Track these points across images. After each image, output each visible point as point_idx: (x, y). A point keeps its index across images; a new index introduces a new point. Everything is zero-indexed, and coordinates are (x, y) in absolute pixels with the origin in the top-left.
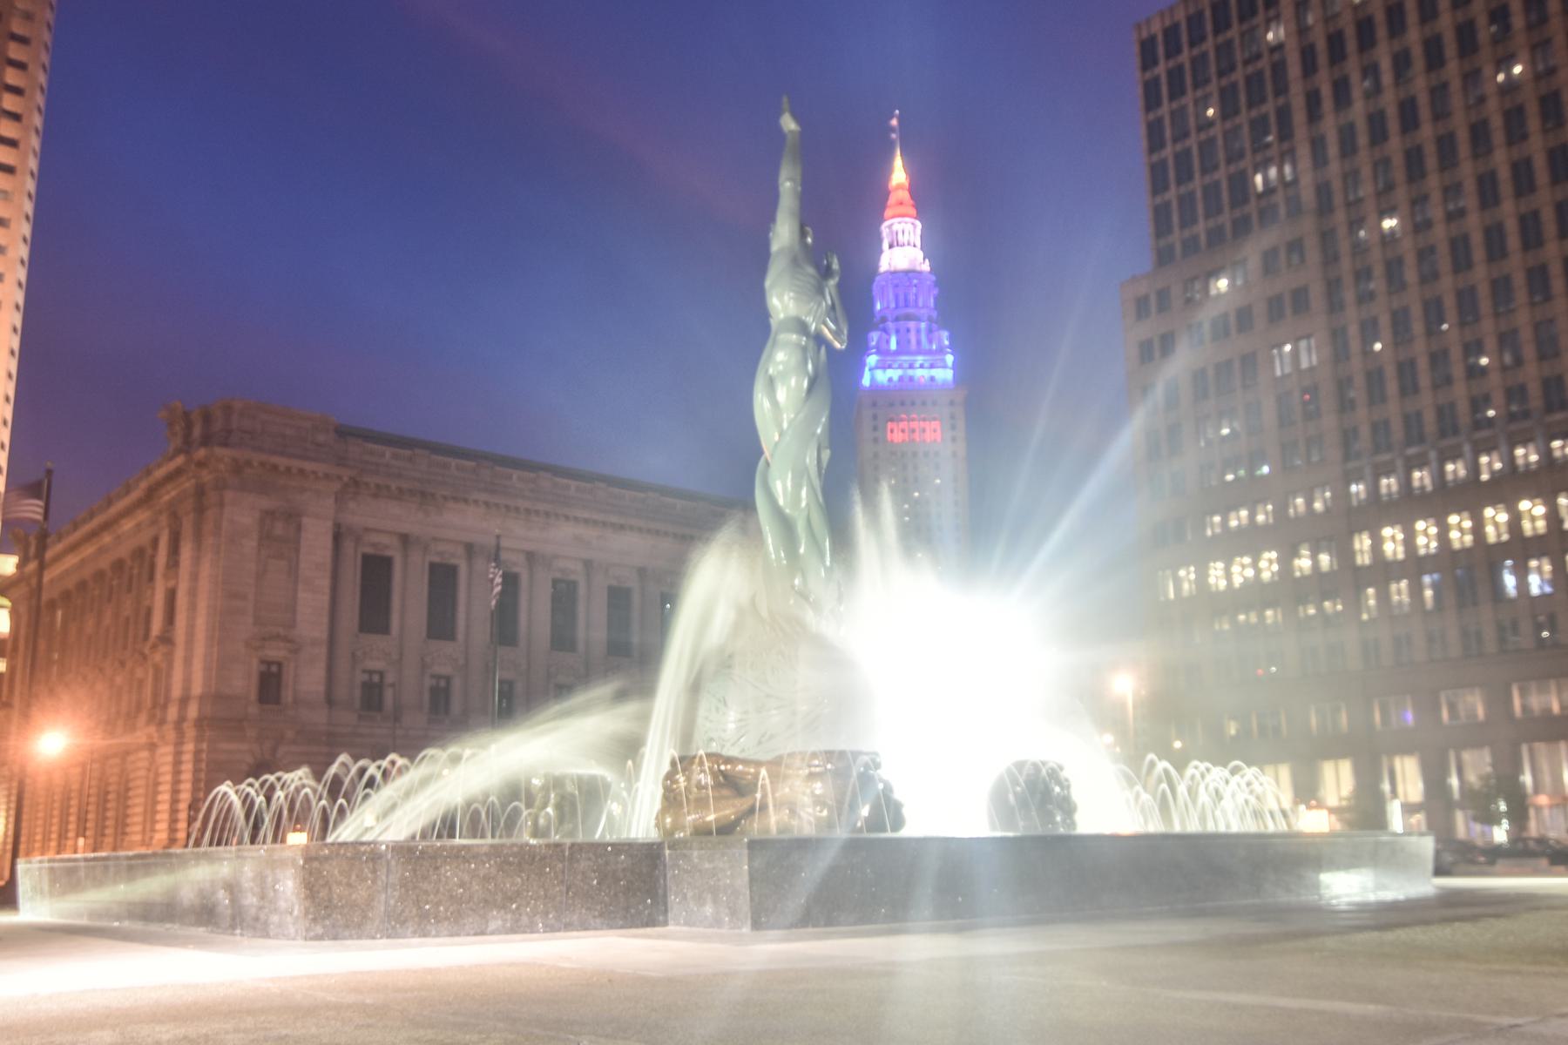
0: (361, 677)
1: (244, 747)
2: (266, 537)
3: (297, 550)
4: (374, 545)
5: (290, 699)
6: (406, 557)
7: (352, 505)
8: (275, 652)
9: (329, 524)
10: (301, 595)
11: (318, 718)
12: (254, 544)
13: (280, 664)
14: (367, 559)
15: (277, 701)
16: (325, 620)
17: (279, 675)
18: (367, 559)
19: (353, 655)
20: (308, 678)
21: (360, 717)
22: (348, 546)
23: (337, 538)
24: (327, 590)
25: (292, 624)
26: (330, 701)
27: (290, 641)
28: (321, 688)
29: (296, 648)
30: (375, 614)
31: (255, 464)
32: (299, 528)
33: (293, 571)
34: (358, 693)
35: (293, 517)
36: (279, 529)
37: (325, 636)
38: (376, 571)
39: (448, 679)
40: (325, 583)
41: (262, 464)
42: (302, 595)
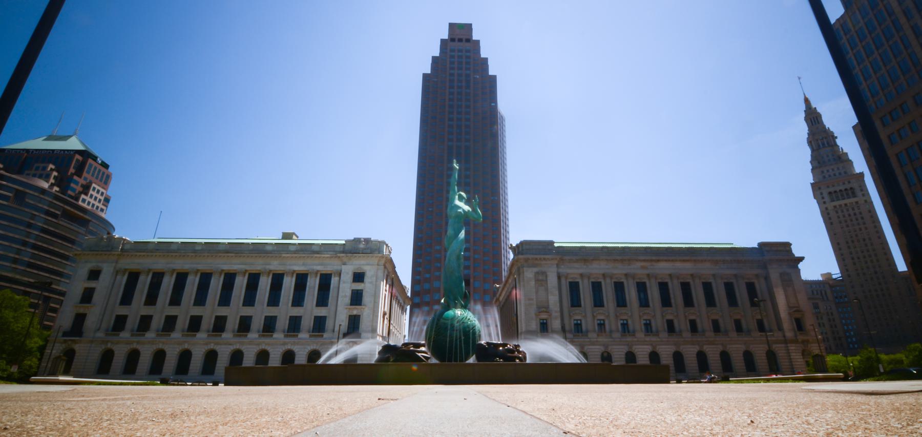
0: (573, 323)
2: (537, 280)
3: (547, 284)
4: (572, 278)
7: (562, 267)
8: (544, 316)
9: (556, 274)
10: (549, 297)
12: (534, 283)
13: (546, 320)
14: (571, 283)
16: (558, 304)
17: (546, 323)
18: (571, 283)
20: (556, 324)
22: (563, 281)
23: (559, 277)
24: (557, 294)
28: (560, 327)
30: (575, 301)
33: (547, 290)
35: (544, 274)
37: (559, 309)
38: (574, 288)
39: (604, 320)
40: (557, 292)
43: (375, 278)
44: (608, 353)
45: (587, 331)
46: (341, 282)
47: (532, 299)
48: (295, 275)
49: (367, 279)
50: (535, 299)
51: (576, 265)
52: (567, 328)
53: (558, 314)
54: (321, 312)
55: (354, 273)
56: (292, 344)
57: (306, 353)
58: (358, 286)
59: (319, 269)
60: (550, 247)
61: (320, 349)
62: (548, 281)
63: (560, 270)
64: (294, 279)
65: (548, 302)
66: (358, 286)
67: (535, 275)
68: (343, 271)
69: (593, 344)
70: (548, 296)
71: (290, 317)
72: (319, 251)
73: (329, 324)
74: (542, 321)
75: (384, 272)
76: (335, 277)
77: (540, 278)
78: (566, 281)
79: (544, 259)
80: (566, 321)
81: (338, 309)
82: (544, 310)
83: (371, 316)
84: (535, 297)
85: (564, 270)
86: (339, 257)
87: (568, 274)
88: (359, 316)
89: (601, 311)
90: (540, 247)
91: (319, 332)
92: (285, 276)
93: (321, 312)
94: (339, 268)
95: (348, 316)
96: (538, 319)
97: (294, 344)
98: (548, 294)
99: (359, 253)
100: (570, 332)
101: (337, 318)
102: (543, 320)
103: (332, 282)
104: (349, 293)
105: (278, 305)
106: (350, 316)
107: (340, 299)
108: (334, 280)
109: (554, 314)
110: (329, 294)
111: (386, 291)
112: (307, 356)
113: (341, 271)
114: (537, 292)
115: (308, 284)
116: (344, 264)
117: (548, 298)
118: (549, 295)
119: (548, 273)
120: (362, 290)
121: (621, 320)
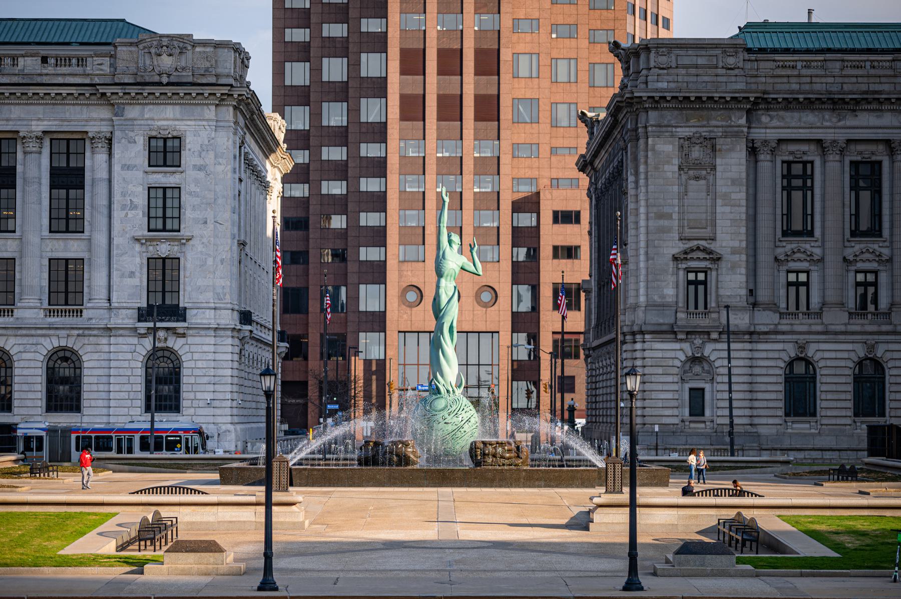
1: (677, 346)
5: (713, 305)
6: (824, 162)
7: (765, 119)
10: (719, 209)
12: (676, 168)
16: (743, 230)
17: (705, 283)
23: (753, 151)
24: (744, 203)
25: (713, 239)
27: (711, 252)
28: (743, 292)
33: (711, 191)
36: (696, 153)
39: (876, 273)
40: (740, 196)
43: (211, 155)
47: (669, 216)
49: (188, 158)
50: (675, 216)
51: (810, 117)
52: (763, 295)
63: (759, 134)
68: (117, 134)
70: (714, 206)
74: (692, 276)
81: (116, 241)
82: (703, 243)
84: (677, 209)
86: (104, 94)
95: (145, 262)
96: (681, 273)
101: (114, 266)
104: (141, 200)
107: (117, 214)
118: (719, 202)
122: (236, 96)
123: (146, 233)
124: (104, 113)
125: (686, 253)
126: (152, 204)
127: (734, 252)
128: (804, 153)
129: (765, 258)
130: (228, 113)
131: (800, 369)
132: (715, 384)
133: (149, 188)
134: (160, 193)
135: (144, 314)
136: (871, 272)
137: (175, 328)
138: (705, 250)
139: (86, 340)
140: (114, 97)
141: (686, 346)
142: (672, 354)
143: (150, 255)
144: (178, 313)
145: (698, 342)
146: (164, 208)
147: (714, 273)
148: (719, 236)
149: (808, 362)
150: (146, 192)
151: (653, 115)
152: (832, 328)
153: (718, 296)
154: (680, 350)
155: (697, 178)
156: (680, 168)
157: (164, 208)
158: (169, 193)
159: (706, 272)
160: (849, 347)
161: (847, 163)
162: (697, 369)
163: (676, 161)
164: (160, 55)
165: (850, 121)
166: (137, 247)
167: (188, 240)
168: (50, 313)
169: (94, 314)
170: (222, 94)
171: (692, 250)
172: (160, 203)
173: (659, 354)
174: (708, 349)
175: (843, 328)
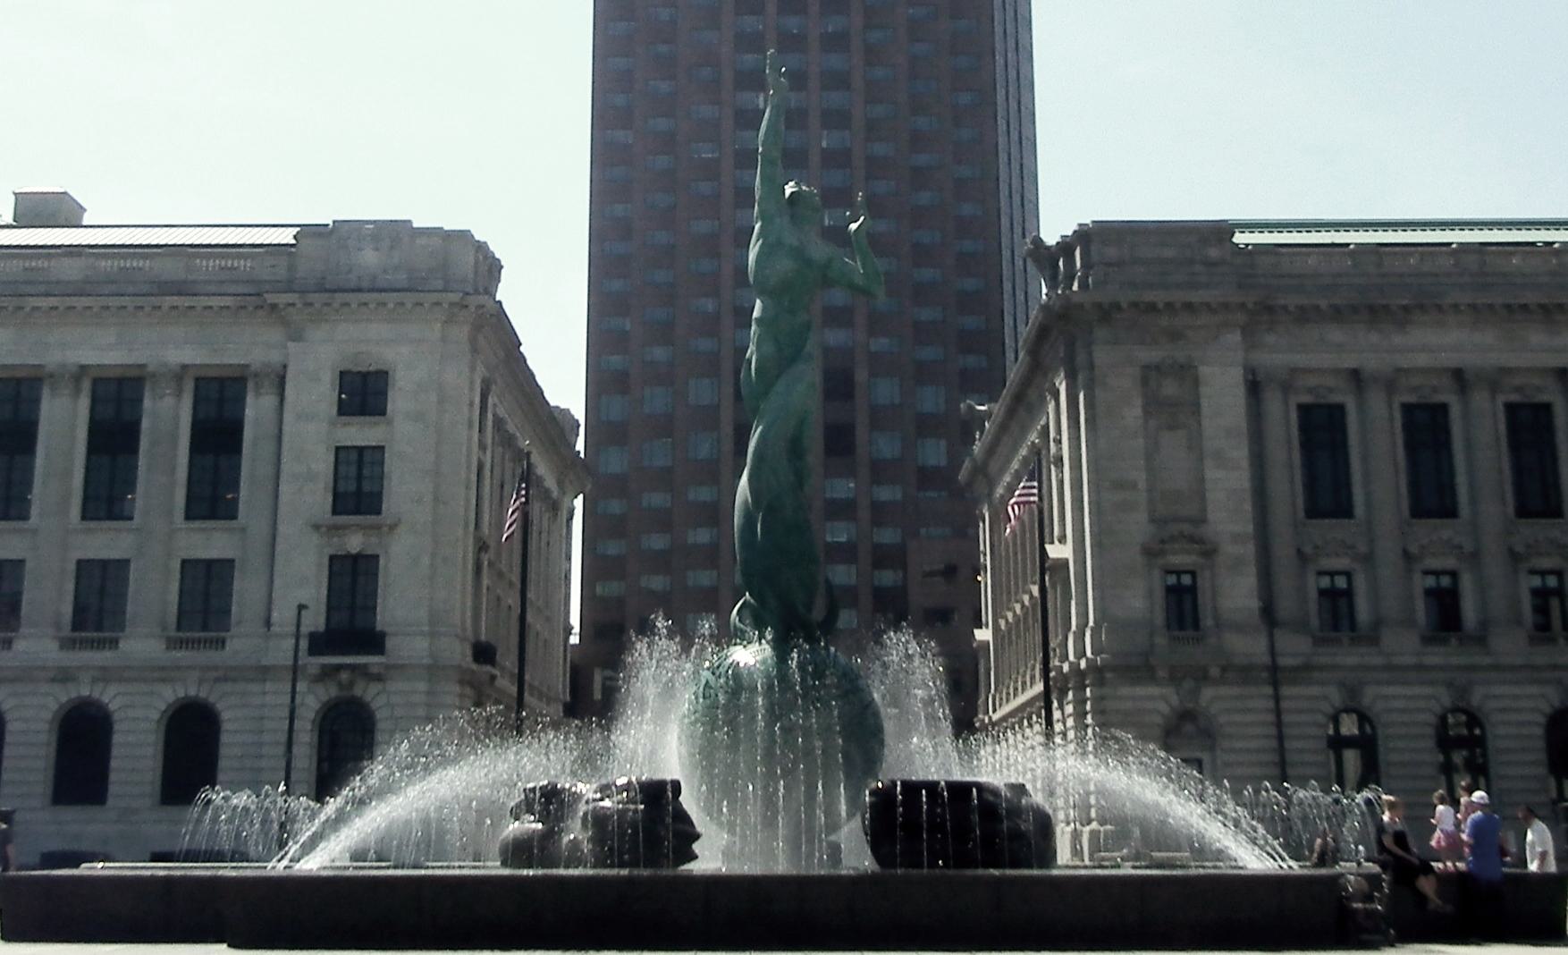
0: (1314, 584)
1: (1153, 690)
2: (1153, 405)
7: (1270, 339)
11: (1251, 647)
12: (1138, 411)
13: (1193, 574)
15: (1196, 625)
17: (1193, 590)
19: (1299, 552)
21: (1319, 642)
23: (1254, 387)
24: (1245, 464)
25: (1201, 520)
26: (1269, 615)
27: (1201, 541)
28: (1255, 604)
29: (1209, 552)
31: (1124, 305)
32: (1196, 382)
34: (1313, 607)
35: (1187, 373)
36: (1170, 388)
37: (1250, 528)
41: (1135, 305)
42: (1212, 473)
43: (433, 398)
44: (1474, 720)
45: (1378, 624)
46: (288, 417)
47: (1134, 486)
48: (86, 385)
49: (398, 401)
50: (1142, 485)
51: (1336, 334)
52: (1286, 606)
53: (1249, 550)
54: (211, 542)
55: (342, 373)
56: (94, 681)
57: (155, 716)
58: (360, 433)
59: (187, 361)
60: (1214, 253)
61: (212, 700)
62: (1204, 403)
64: (84, 404)
65: (1200, 494)
66: (360, 433)
67: (1145, 381)
69: (1395, 672)
71: (79, 562)
72: (185, 282)
73: (246, 592)
74: (1172, 580)
75: (473, 369)
76: (258, 394)
77: (1170, 388)
78: (1286, 403)
79: (1189, 307)
80: (1285, 582)
81: (281, 528)
82: (1187, 528)
83: (426, 560)
85: (1278, 353)
87: (1294, 371)
88: (378, 556)
89: (1446, 534)
90: (1169, 253)
91: (205, 628)
92: (46, 393)
93: (211, 542)
94: (275, 357)
95: (326, 561)
96: (1157, 574)
97: (105, 675)
98: (1201, 459)
99: (359, 290)
100: (1301, 626)
101: (278, 567)
102: (1178, 573)
103: (249, 412)
104: (323, 465)
105: (24, 516)
106: (332, 558)
108: (256, 409)
109: (1229, 549)
110: (238, 467)
111: (482, 447)
112: (163, 728)
113: (285, 367)
114: (1150, 455)
115: (145, 424)
116: (297, 336)
117: (1202, 480)
118: (1208, 463)
119: (1204, 370)
120: (381, 449)
121: (1533, 572)
122: (473, 309)
123: (328, 515)
124: (275, 335)
125: (1163, 542)
126: (342, 469)
127: (1237, 538)
128: (1331, 390)
129: (1283, 550)
130: (461, 333)
131: (1349, 727)
132: (1219, 753)
133: (338, 449)
134: (354, 456)
135: (320, 644)
136: (1444, 572)
137: (365, 666)
138: (1192, 539)
139: (227, 687)
140: (291, 309)
141: (1169, 691)
142: (1150, 705)
143: (333, 552)
144: (373, 641)
145: (1188, 684)
146: (360, 477)
147: (1207, 574)
148: (1211, 516)
149: (1363, 718)
150: (332, 458)
151: (1101, 333)
152: (1397, 660)
153: (1215, 608)
154: (1164, 698)
155: (1171, 428)
156: (1147, 413)
157: (360, 477)
158: (367, 457)
159: (1193, 574)
160: (1427, 690)
161: (1396, 406)
162: (1189, 728)
163: (1138, 402)
164: (360, 249)
165: (1398, 339)
166: (315, 539)
167: (392, 527)
168: (173, 644)
169: (241, 645)
170: (452, 304)
171: (1172, 539)
172: (353, 470)
173: (1129, 705)
174: (1208, 693)
175: (1409, 660)
